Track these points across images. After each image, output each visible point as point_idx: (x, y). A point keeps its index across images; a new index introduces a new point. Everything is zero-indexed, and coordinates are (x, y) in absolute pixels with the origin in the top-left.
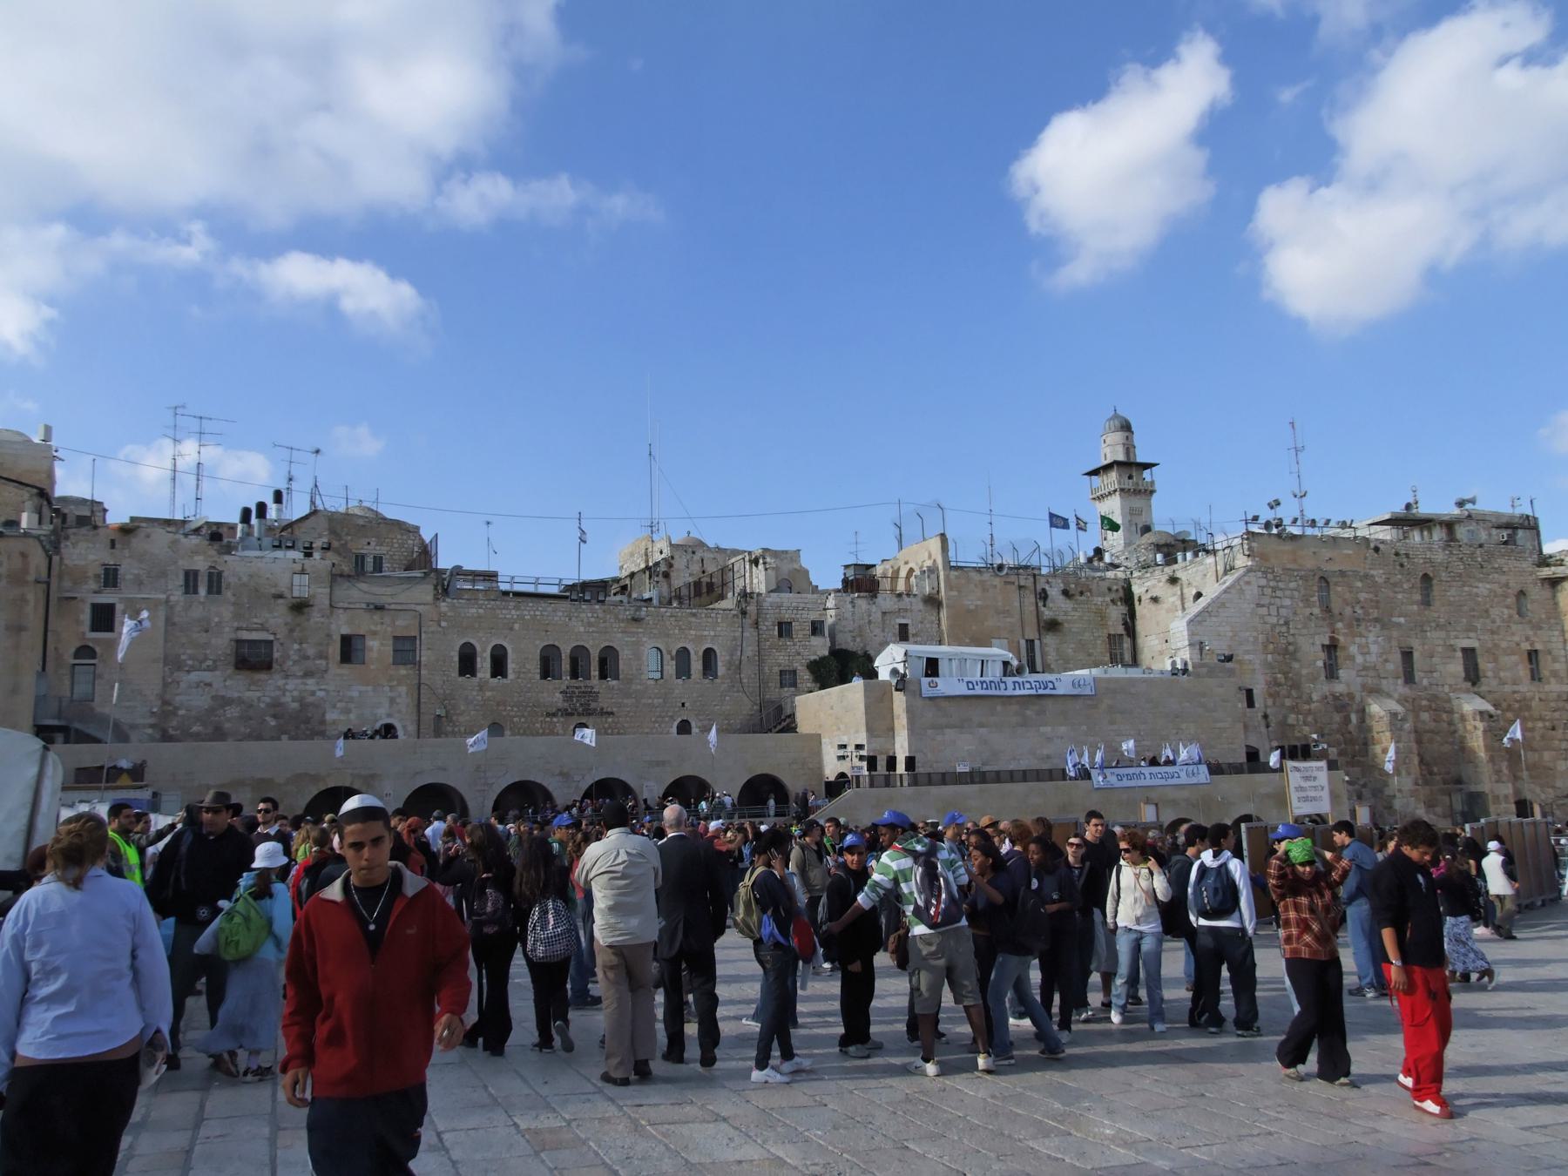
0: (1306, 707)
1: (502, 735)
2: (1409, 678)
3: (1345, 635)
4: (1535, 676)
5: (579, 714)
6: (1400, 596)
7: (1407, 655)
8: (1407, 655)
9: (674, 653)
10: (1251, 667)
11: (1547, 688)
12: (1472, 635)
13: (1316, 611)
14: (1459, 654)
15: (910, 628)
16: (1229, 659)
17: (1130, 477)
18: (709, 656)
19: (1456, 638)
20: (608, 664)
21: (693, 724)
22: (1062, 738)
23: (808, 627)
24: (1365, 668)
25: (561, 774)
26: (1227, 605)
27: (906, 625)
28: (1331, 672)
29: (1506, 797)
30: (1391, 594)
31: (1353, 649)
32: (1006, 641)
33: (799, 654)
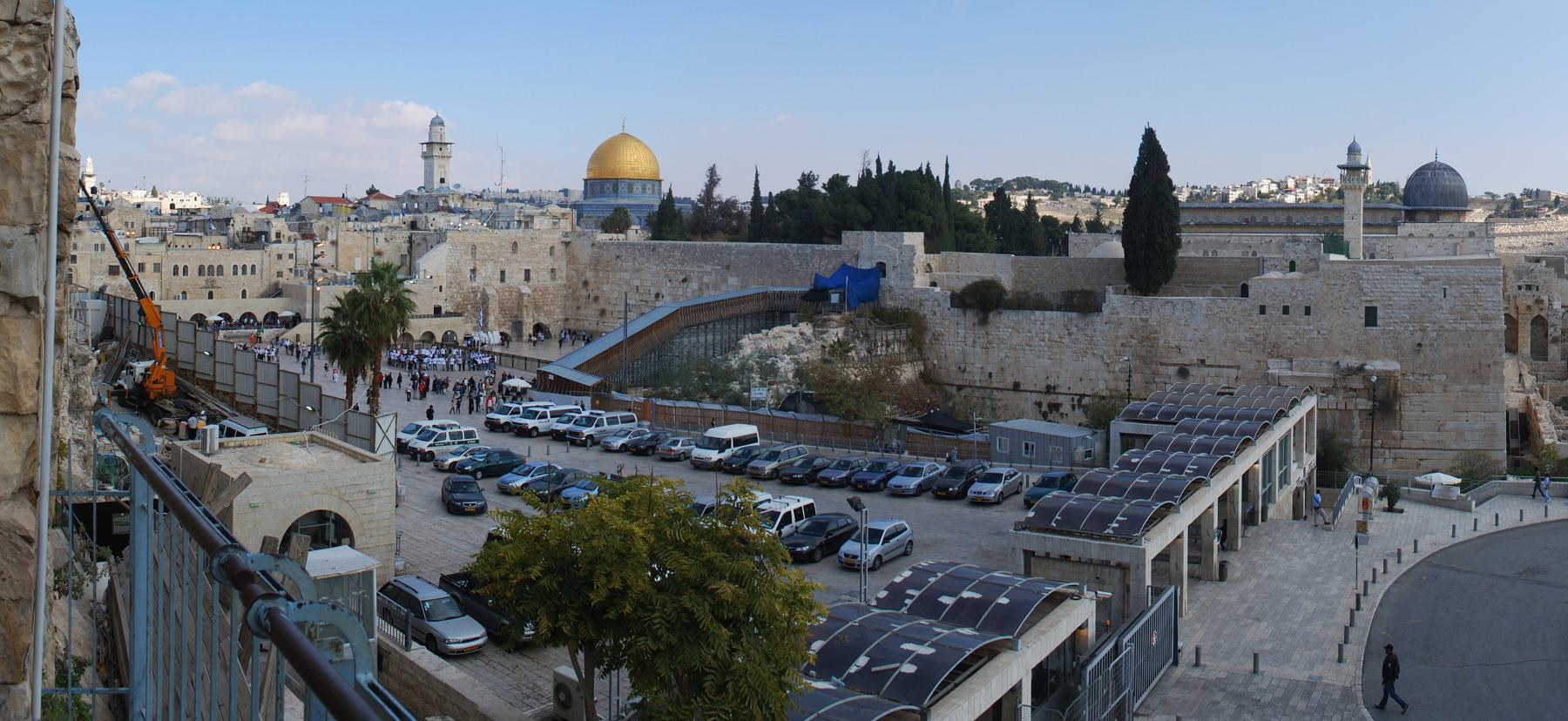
2: (502, 280)
4: (553, 278)
7: (503, 273)
8: (503, 273)
18: (253, 267)
28: (473, 279)
31: (482, 271)
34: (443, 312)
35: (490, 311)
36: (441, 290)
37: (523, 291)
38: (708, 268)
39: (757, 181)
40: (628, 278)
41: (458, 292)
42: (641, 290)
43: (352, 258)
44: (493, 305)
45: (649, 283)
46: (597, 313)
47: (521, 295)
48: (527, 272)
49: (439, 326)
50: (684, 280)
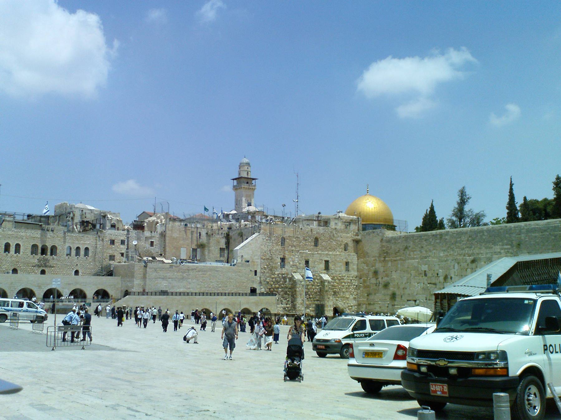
0: (273, 276)
1: (17, 273)
3: (288, 255)
4: (347, 270)
5: (43, 267)
6: (307, 243)
9: (75, 248)
10: (257, 263)
11: (350, 273)
12: (328, 256)
13: (280, 247)
14: (324, 262)
15: (154, 242)
16: (248, 261)
17: (247, 183)
18: (87, 249)
19: (323, 257)
20: (54, 250)
21: (80, 271)
22: (194, 283)
23: (120, 241)
24: (293, 265)
25: (38, 286)
26: (252, 244)
27: (153, 242)
28: (283, 266)
29: (330, 306)
30: (305, 243)
32: (186, 249)
33: (116, 250)
34: (258, 291)
35: (298, 293)
36: (256, 274)
37: (324, 278)
38: (497, 248)
39: (511, 189)
40: (416, 265)
41: (270, 277)
42: (429, 275)
43: (178, 249)
44: (300, 289)
45: (437, 267)
46: (388, 298)
47: (323, 282)
48: (327, 262)
49: (257, 304)
50: (473, 261)
